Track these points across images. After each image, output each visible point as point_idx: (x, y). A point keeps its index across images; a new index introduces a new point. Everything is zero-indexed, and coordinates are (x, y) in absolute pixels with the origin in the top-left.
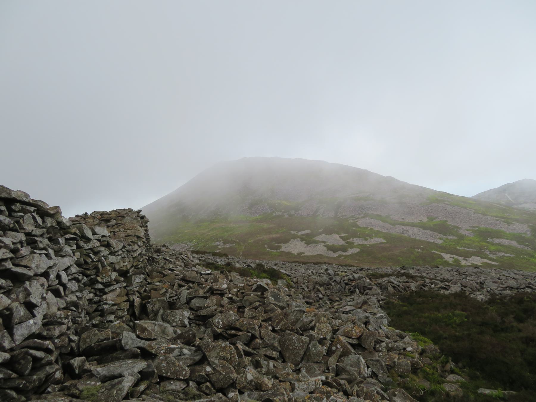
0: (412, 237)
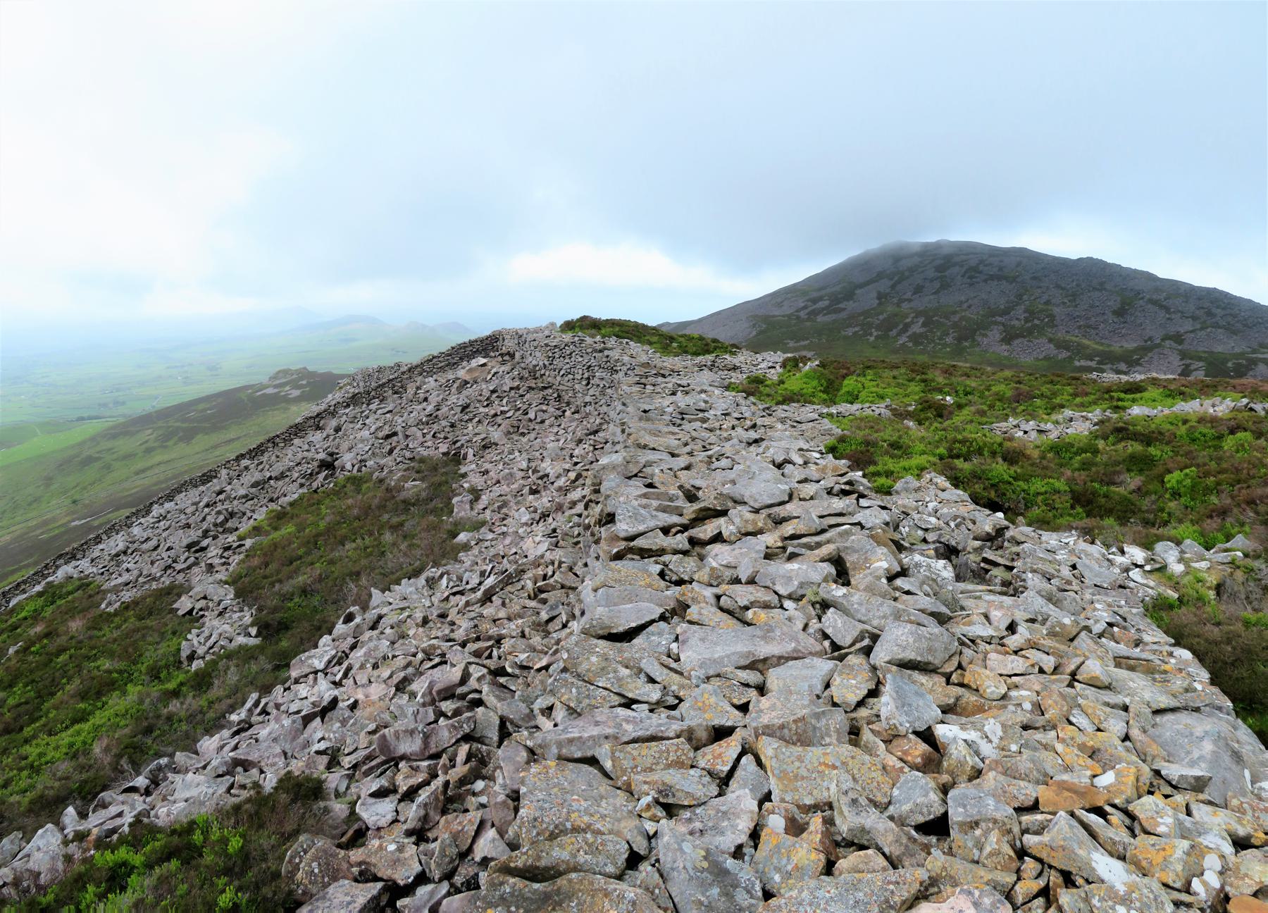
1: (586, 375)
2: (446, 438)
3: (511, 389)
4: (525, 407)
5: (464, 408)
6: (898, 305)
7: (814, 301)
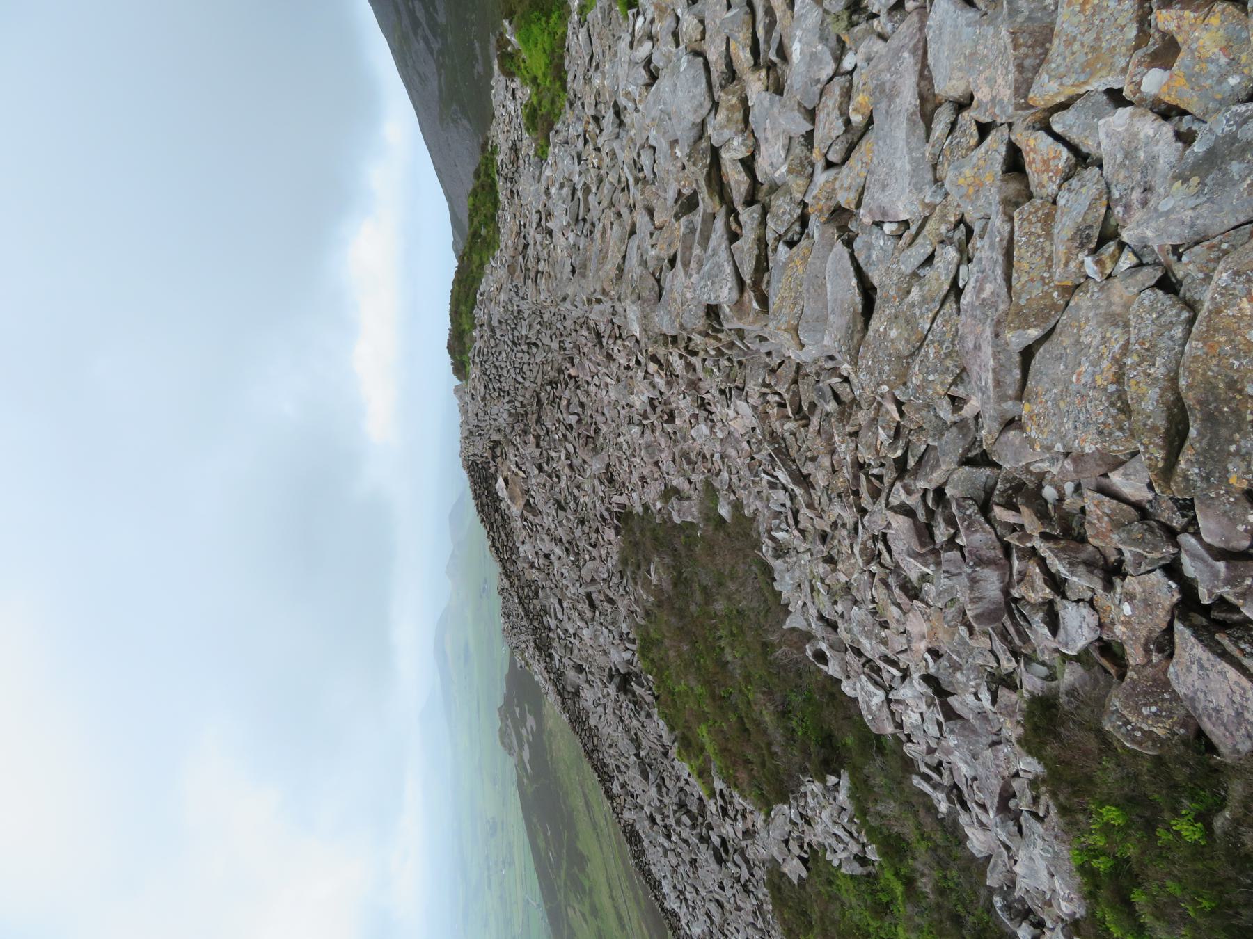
1: (525, 347)
2: (597, 531)
3: (538, 445)
4: (562, 428)
5: (560, 506)
7: (415, 24)
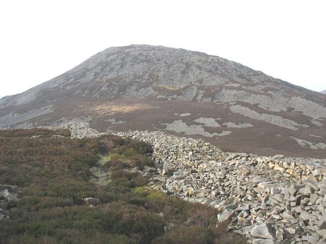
0: (274, 123)
6: (102, 78)
